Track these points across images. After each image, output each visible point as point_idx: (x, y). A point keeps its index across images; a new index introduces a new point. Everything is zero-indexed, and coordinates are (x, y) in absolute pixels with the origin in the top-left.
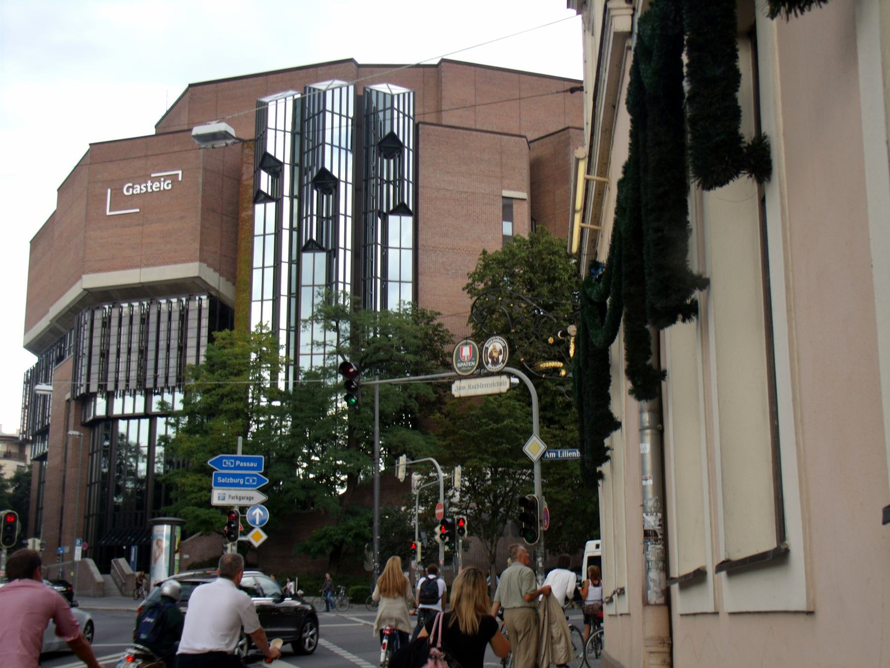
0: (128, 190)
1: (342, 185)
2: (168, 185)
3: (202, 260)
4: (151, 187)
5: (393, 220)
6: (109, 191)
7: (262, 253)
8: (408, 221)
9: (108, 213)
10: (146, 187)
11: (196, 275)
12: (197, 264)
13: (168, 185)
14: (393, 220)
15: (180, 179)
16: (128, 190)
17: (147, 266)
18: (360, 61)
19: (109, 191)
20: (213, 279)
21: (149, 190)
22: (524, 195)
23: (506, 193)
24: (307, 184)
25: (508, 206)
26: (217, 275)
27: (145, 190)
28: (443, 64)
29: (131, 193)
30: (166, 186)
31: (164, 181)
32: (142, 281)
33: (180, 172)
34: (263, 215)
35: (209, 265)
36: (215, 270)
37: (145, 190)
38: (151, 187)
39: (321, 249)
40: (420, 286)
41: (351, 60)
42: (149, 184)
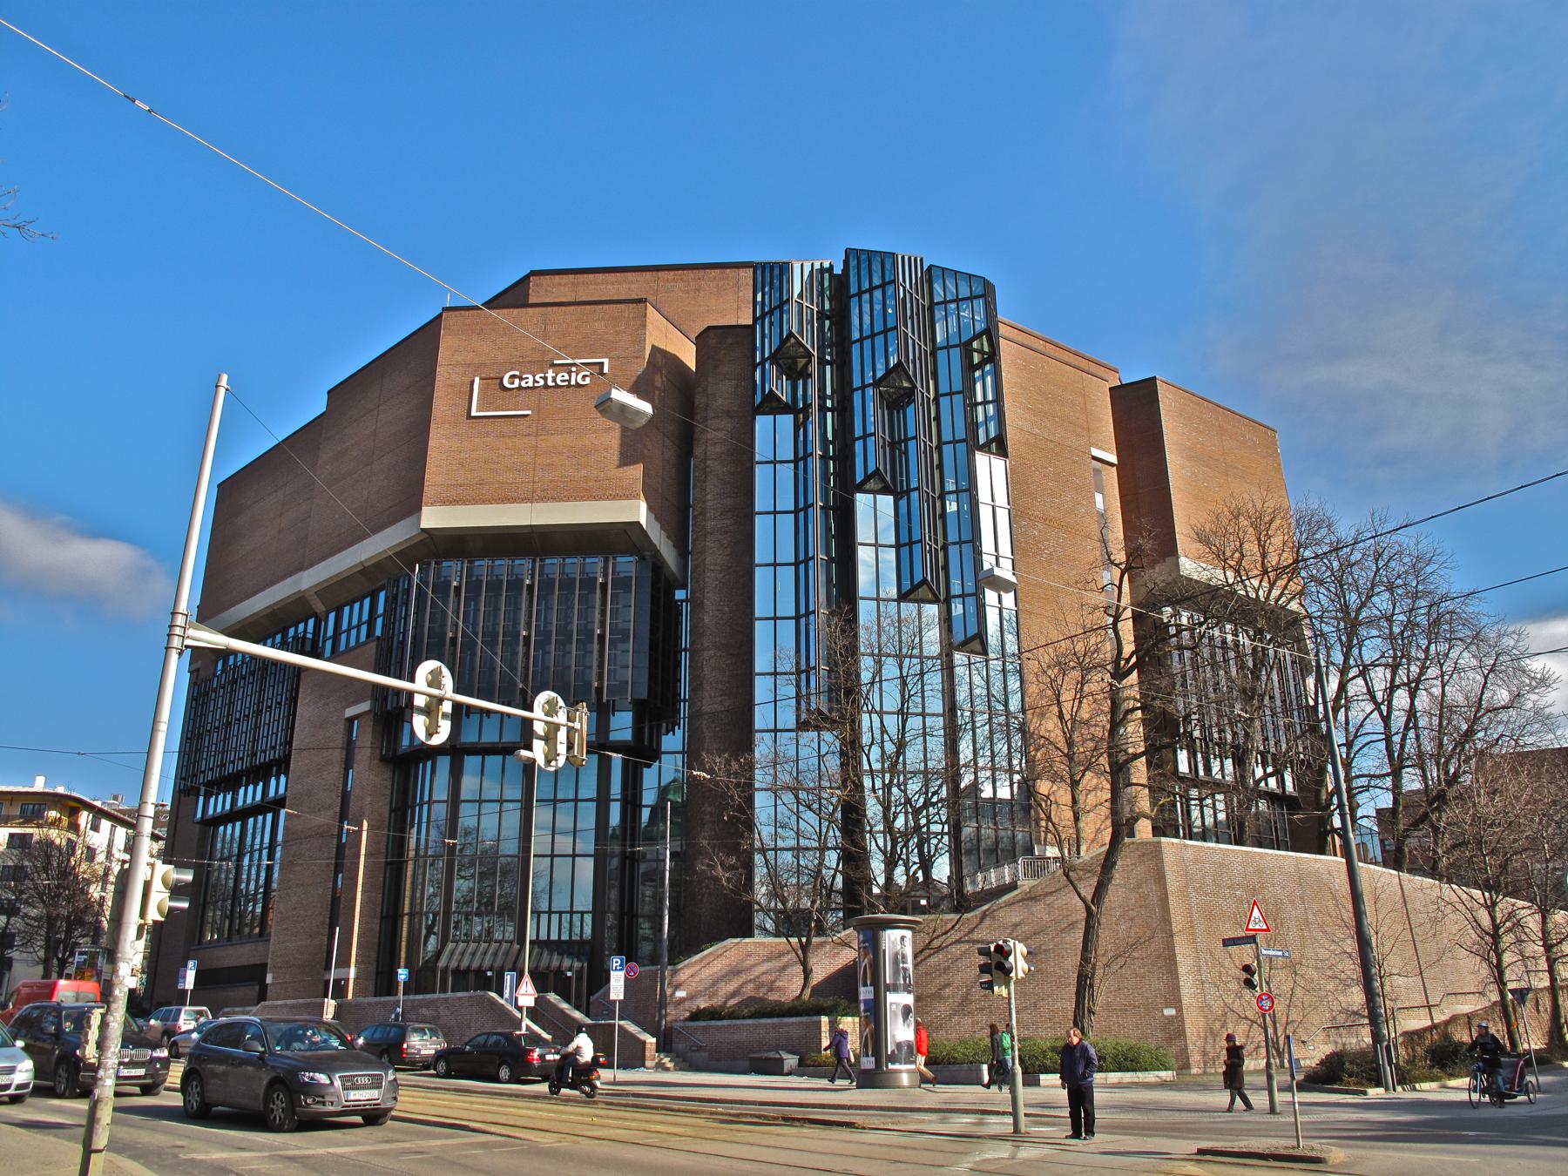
4: (554, 380)
5: (981, 459)
6: (477, 380)
7: (773, 488)
8: (999, 464)
9: (474, 413)
10: (545, 379)
14: (981, 459)
15: (606, 370)
17: (542, 500)
19: (477, 380)
21: (550, 383)
22: (1113, 459)
27: (542, 382)
29: (516, 384)
33: (606, 361)
34: (772, 435)
37: (542, 382)
38: (554, 380)
39: (886, 490)
42: (550, 374)
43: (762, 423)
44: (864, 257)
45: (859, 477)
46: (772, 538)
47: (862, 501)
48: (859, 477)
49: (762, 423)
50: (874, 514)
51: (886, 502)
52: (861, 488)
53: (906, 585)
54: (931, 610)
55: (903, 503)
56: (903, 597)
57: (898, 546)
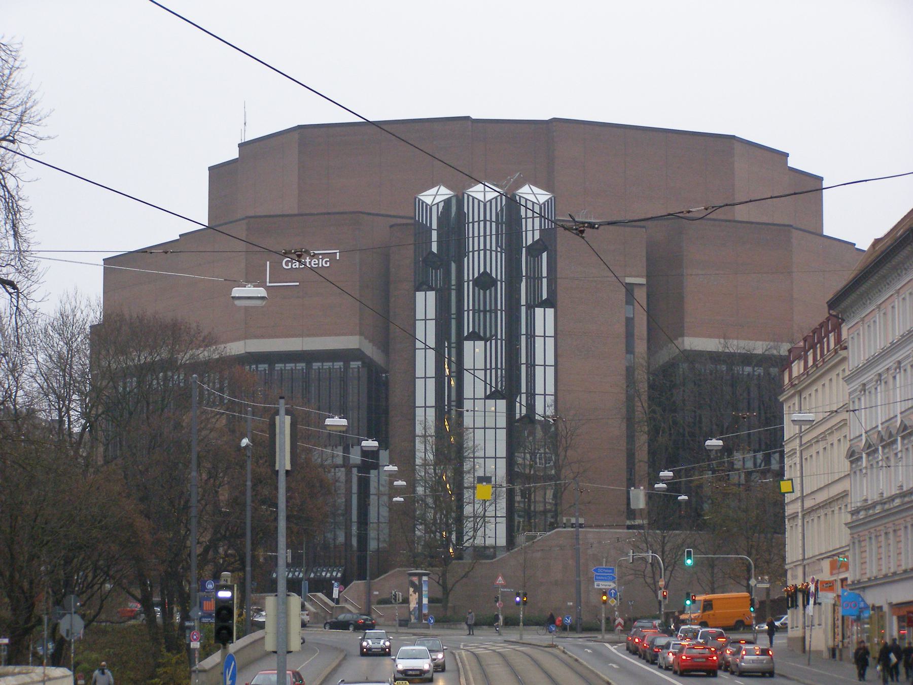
0: (287, 265)
1: (499, 283)
2: (326, 262)
3: (361, 334)
4: (310, 263)
5: (539, 311)
8: (550, 312)
9: (268, 284)
11: (356, 346)
12: (357, 337)
13: (326, 262)
14: (539, 311)
16: (287, 265)
17: (308, 336)
18: (473, 117)
20: (370, 350)
22: (643, 281)
23: (629, 280)
24: (468, 281)
25: (630, 289)
26: (371, 344)
28: (554, 124)
30: (324, 263)
31: (322, 259)
32: (305, 349)
35: (366, 338)
36: (370, 341)
38: (310, 263)
39: (480, 339)
40: (559, 367)
41: (468, 118)
43: (420, 296)
44: (471, 198)
45: (466, 334)
46: (425, 363)
47: (468, 345)
48: (466, 334)
49: (420, 296)
50: (475, 353)
51: (480, 344)
52: (469, 338)
53: (488, 393)
54: (502, 404)
55: (488, 343)
56: (487, 397)
57: (485, 370)
